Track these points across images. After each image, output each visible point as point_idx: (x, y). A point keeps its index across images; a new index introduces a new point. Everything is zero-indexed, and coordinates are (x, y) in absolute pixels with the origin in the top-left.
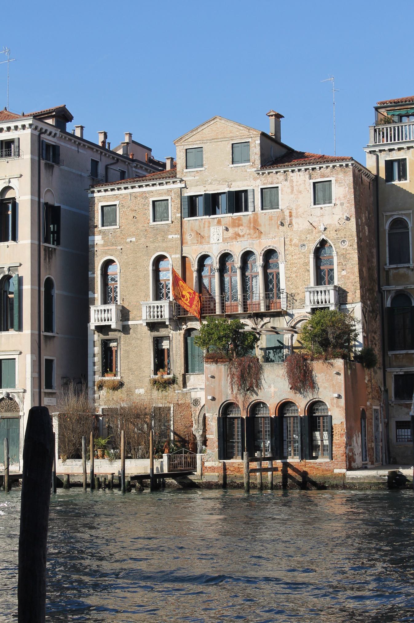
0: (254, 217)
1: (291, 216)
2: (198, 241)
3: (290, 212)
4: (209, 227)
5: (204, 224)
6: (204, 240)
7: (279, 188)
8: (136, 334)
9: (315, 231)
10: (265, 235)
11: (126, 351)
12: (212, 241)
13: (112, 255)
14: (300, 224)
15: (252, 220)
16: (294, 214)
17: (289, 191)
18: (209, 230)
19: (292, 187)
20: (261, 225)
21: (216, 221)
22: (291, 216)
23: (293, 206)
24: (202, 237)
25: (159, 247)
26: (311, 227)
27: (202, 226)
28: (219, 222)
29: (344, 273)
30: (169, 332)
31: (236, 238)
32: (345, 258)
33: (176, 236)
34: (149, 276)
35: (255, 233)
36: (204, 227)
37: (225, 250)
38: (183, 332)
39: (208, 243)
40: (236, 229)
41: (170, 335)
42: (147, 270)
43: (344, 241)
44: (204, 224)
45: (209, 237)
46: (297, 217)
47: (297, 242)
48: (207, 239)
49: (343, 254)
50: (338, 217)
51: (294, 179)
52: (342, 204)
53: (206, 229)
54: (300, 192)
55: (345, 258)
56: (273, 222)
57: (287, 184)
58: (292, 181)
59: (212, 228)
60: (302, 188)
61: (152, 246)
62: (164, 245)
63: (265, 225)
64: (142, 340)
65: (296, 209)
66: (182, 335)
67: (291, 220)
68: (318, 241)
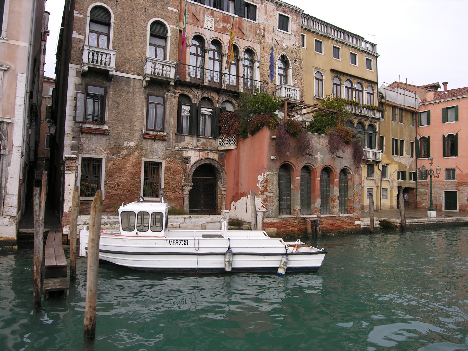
0: (239, 21)
1: (264, 30)
2: (194, 21)
3: (264, 28)
4: (204, 14)
5: (200, 10)
6: (199, 23)
7: (257, 7)
8: (128, 88)
9: (279, 47)
10: (246, 37)
11: (115, 101)
12: (205, 26)
13: (105, 3)
14: (269, 39)
15: (238, 22)
16: (266, 30)
17: (264, 12)
18: (204, 16)
19: (266, 10)
20: (243, 29)
21: (209, 12)
22: (264, 30)
23: (266, 24)
24: (198, 20)
25: (158, 13)
26: (276, 43)
27: (198, 11)
28: (212, 14)
29: (296, 82)
30: (164, 93)
31: (225, 31)
32: (296, 71)
33: (175, 10)
34: (146, 36)
35: (239, 33)
36: (200, 13)
37: (216, 37)
38: (178, 95)
39: (203, 27)
40: (226, 25)
41: (165, 96)
42: (144, 30)
43: (296, 61)
44: (200, 10)
45: (203, 21)
46: (268, 33)
47: (268, 50)
48: (202, 23)
49: (295, 69)
50: (293, 43)
51: (267, 5)
52: (295, 36)
53: (201, 15)
54: (271, 16)
55: (296, 71)
56: (252, 29)
57: (263, 6)
58: (266, 6)
59: (206, 16)
60: (272, 14)
61: (151, 10)
62: (163, 13)
63: (246, 29)
64: (134, 94)
65: (268, 27)
66: (177, 99)
67: (264, 33)
68: (280, 55)
